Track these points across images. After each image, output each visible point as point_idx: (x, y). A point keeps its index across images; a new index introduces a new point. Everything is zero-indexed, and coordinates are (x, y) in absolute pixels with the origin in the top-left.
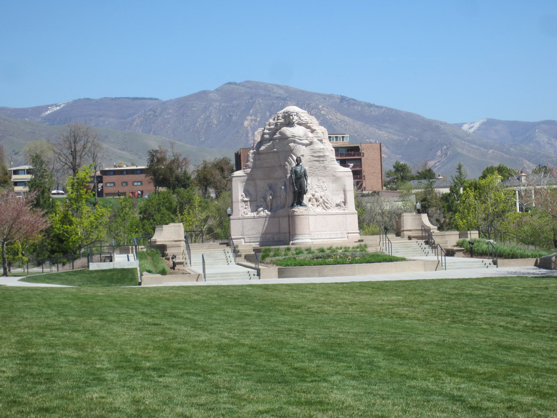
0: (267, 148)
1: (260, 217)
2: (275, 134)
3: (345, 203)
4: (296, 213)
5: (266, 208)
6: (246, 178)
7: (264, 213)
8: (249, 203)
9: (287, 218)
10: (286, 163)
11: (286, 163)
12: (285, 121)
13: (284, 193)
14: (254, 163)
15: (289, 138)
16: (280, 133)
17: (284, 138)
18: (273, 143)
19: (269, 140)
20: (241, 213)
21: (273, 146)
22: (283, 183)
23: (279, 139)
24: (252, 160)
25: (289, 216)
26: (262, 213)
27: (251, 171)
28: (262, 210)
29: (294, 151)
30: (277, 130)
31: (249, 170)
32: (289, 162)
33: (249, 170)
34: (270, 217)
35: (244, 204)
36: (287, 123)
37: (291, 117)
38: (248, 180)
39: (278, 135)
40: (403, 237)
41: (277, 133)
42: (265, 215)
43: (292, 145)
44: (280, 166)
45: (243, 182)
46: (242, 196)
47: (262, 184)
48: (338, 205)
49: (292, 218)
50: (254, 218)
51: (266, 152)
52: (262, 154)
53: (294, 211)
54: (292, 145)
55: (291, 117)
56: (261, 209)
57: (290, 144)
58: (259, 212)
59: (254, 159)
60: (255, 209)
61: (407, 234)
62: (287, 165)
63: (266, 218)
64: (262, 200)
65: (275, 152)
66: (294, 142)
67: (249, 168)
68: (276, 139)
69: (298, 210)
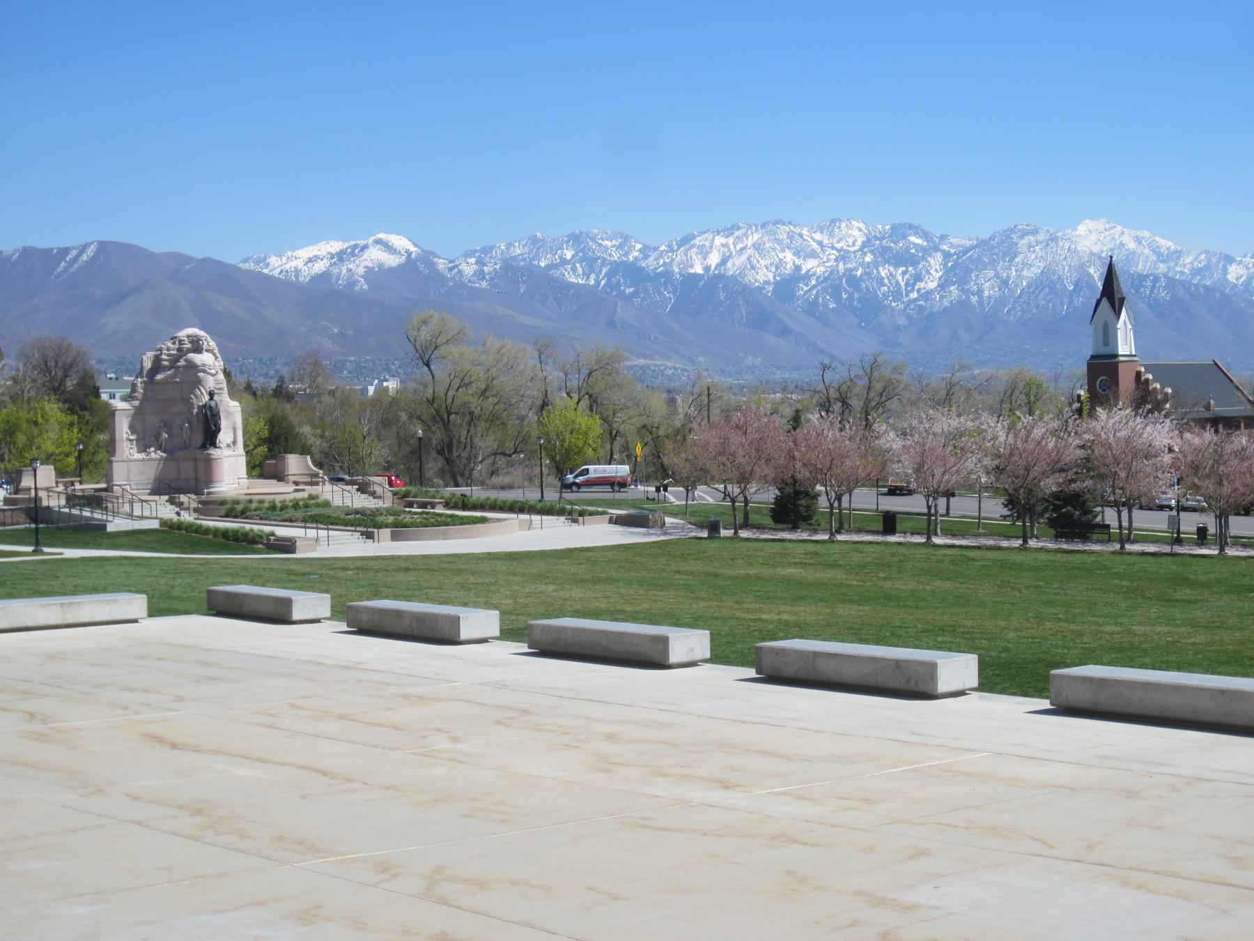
0: (166, 378)
1: (151, 460)
2: (178, 360)
3: (234, 443)
5: (159, 448)
7: (155, 454)
14: (144, 395)
16: (186, 360)
17: (192, 366)
19: (170, 368)
20: (127, 453)
21: (175, 376)
23: (184, 367)
30: (181, 357)
31: (137, 403)
34: (166, 460)
39: (182, 363)
40: (287, 482)
43: (201, 374)
47: (153, 420)
48: (228, 445)
49: (209, 461)
50: (143, 460)
51: (164, 382)
54: (201, 374)
58: (149, 453)
59: (145, 389)
60: (143, 448)
61: (292, 478)
66: (204, 371)
69: (214, 452)
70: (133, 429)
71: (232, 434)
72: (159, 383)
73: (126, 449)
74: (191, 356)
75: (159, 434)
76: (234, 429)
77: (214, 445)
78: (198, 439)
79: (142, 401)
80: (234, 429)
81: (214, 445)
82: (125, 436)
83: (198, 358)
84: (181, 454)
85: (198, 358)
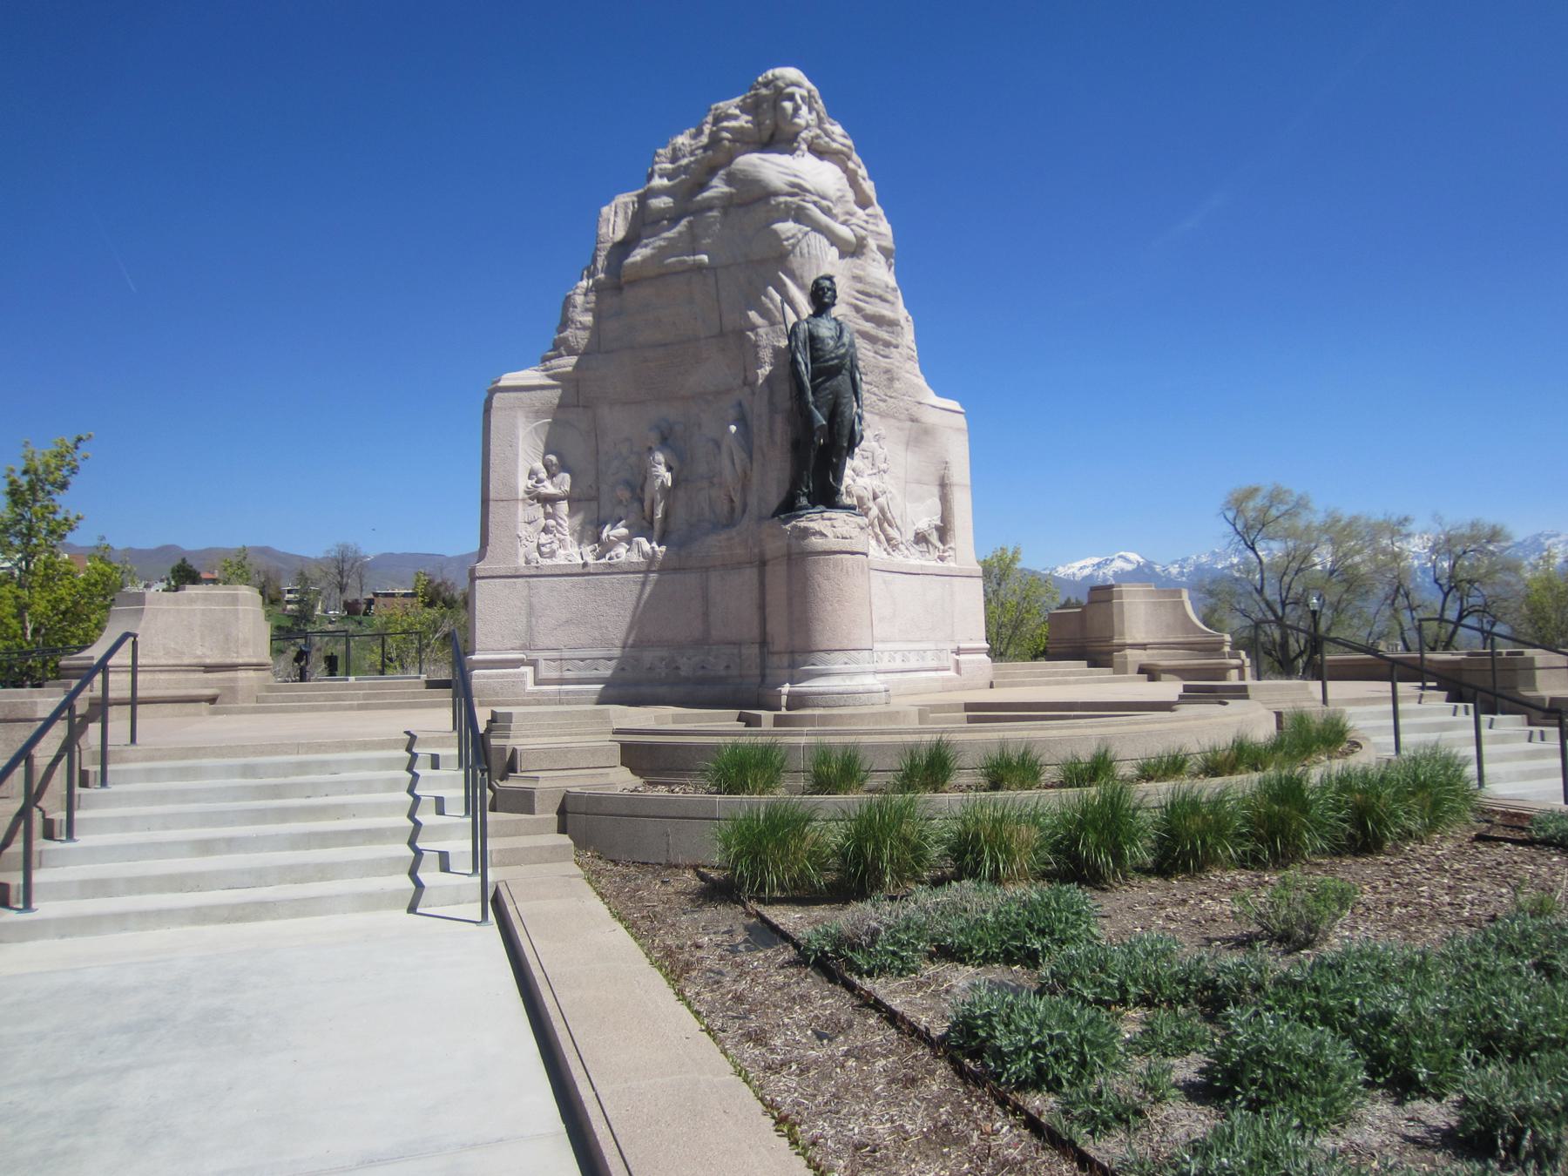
0: (662, 253)
1: (612, 570)
2: (703, 186)
3: (944, 531)
4: (816, 541)
5: (643, 527)
6: (554, 396)
7: (634, 550)
8: (563, 506)
9: (751, 574)
10: (753, 314)
11: (753, 314)
12: (758, 124)
13: (739, 456)
14: (596, 330)
15: (776, 194)
16: (730, 180)
17: (755, 198)
18: (691, 225)
19: (675, 221)
20: (526, 550)
22: (732, 413)
23: (727, 204)
24: (588, 319)
25: (763, 563)
26: (622, 550)
27: (577, 367)
28: (620, 539)
29: (795, 262)
30: (712, 172)
31: (568, 363)
32: (765, 313)
33: (568, 363)
35: (538, 511)
36: (766, 135)
37: (788, 105)
38: (562, 405)
39: (718, 187)
40: (1122, 669)
41: (716, 182)
42: (635, 557)
43: (787, 228)
44: (722, 334)
45: (538, 414)
46: (532, 474)
48: (921, 538)
49: (800, 560)
50: (584, 571)
51: (656, 274)
52: (633, 283)
53: (806, 533)
54: (787, 228)
55: (788, 105)
56: (621, 531)
57: (778, 226)
58: (605, 547)
59: (598, 315)
60: (591, 532)
61: (1135, 657)
62: (754, 328)
63: (647, 572)
64: (624, 494)
65: (699, 267)
66: (800, 216)
67: (571, 352)
68: (709, 206)
70: (558, 455)
71: (934, 504)
72: (640, 278)
74: (751, 161)
75: (645, 475)
76: (944, 485)
77: (828, 497)
79: (585, 355)
80: (944, 485)
81: (828, 497)
82: (523, 483)
83: (772, 168)
84: (715, 544)
85: (772, 168)
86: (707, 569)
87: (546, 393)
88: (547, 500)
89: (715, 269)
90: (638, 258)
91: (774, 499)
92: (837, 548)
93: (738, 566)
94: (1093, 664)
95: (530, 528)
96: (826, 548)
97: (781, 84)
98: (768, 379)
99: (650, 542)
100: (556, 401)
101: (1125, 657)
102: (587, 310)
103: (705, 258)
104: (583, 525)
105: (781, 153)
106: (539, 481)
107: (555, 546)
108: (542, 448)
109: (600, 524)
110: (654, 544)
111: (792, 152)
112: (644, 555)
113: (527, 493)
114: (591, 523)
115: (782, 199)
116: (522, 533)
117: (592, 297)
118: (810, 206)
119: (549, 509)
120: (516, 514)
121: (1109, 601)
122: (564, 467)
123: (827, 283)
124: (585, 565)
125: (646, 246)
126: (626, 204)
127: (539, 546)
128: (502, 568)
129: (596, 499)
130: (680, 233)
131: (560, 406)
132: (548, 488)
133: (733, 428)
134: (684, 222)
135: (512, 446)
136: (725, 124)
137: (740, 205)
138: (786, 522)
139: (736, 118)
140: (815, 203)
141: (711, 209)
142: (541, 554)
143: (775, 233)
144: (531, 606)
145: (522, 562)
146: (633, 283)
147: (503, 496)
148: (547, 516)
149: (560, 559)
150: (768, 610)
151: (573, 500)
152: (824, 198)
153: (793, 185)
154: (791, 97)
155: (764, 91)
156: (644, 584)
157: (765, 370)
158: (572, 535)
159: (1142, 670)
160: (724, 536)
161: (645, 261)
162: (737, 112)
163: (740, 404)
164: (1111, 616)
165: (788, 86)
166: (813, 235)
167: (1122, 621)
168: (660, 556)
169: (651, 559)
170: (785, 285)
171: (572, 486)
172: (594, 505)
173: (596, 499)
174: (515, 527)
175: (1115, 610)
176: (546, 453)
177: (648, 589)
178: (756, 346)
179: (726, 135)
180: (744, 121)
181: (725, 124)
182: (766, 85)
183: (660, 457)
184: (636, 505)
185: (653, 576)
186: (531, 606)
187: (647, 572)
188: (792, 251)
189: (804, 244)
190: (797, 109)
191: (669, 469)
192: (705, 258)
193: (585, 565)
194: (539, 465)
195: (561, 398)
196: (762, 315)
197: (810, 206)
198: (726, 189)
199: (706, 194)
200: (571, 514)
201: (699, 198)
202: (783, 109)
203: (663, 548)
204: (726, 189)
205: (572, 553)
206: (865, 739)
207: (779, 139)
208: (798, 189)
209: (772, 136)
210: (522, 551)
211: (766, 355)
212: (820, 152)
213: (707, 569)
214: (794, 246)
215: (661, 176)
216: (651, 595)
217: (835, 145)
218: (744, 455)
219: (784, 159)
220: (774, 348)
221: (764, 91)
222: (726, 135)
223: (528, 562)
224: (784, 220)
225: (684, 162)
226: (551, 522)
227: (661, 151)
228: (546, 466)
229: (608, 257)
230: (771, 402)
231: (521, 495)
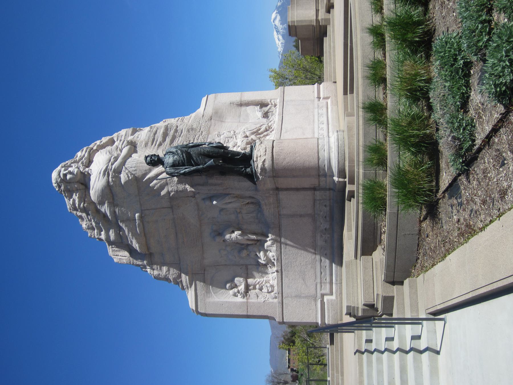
1: (279, 259)
2: (105, 215)
3: (263, 105)
4: (267, 164)
5: (260, 244)
6: (200, 284)
7: (271, 249)
8: (250, 281)
9: (282, 195)
10: (163, 193)
11: (163, 193)
12: (77, 190)
13: (227, 200)
14: (170, 265)
15: (108, 182)
16: (102, 203)
17: (110, 192)
19: (120, 229)
22: (208, 203)
23: (113, 204)
24: (165, 269)
25: (277, 189)
26: (270, 254)
27: (186, 274)
28: (265, 255)
29: (139, 174)
30: (98, 211)
31: (185, 278)
32: (162, 188)
33: (185, 278)
34: (279, 234)
35: (252, 293)
36: (82, 187)
37: (69, 177)
39: (105, 209)
40: (328, 21)
41: (103, 210)
42: (274, 248)
43: (123, 178)
44: (171, 207)
45: (208, 292)
46: (235, 295)
48: (266, 115)
49: (276, 172)
50: (280, 272)
51: (144, 237)
52: (148, 249)
53: (263, 169)
54: (123, 178)
55: (69, 177)
56: (262, 254)
57: (123, 182)
58: (269, 262)
60: (262, 268)
61: (322, 14)
62: (169, 193)
63: (281, 243)
64: (244, 253)
65: (141, 217)
66: (118, 171)
67: (180, 276)
68: (114, 213)
69: (261, 159)
70: (225, 283)
71: (250, 109)
73: (261, 299)
74: (94, 193)
76: (242, 104)
77: (246, 159)
78: (237, 184)
79: (181, 270)
80: (242, 104)
81: (246, 159)
82: (239, 299)
83: (97, 184)
84: (268, 212)
85: (97, 184)
86: (279, 215)
87: (198, 288)
88: (247, 288)
89: (142, 210)
90: (137, 245)
91: (247, 184)
92: (271, 154)
93: (278, 201)
94: (325, 34)
95: (260, 296)
96: (270, 159)
97: (59, 180)
98: (192, 186)
99: (266, 241)
100: (202, 283)
101: (322, 19)
102: (161, 269)
103: (137, 215)
104: (259, 272)
105: (90, 180)
106: (238, 292)
107: (268, 285)
108: (223, 290)
109: (258, 264)
110: (268, 239)
111: (90, 175)
112: (273, 244)
113: (244, 297)
114: (258, 268)
115: (110, 180)
116: (263, 300)
117: (155, 267)
118: (113, 167)
119: (251, 287)
120: (253, 303)
121: (296, 27)
122: (232, 281)
123: (148, 159)
124: (277, 271)
125: (132, 242)
126: (113, 251)
127: (268, 292)
128: (278, 310)
129: (247, 266)
130: (126, 226)
131: (204, 282)
132: (242, 288)
133: (215, 202)
134: (121, 224)
135: (222, 304)
136: (77, 205)
137: (113, 199)
138: (258, 178)
139: (74, 201)
140: (112, 164)
141: (115, 212)
142: (272, 291)
143: (126, 182)
144: (296, 296)
145: (276, 300)
146: (148, 249)
147: (245, 308)
148: (255, 288)
149: (275, 283)
150: (299, 187)
151: (247, 277)
152: (110, 160)
153: (104, 174)
154: (65, 175)
155: (62, 188)
156: (286, 244)
157: (188, 188)
158: (263, 277)
159: (328, 11)
160: (264, 207)
161: (138, 242)
162: (72, 200)
163: (204, 199)
164: (302, 26)
165: (60, 177)
166: (126, 166)
167: (305, 21)
168: (273, 237)
169: (274, 241)
170: (149, 178)
171: (241, 277)
172: (249, 267)
173: (247, 266)
174: (259, 303)
175: (300, 24)
176: (226, 288)
177: (289, 242)
178: (177, 192)
179: (82, 205)
180: (76, 197)
181: (77, 205)
182: (60, 187)
183: (227, 236)
184: (250, 248)
185: (283, 240)
186: (296, 296)
187: (281, 243)
188: (134, 175)
189: (131, 170)
190: (70, 173)
191: (233, 232)
192: (137, 215)
193: (277, 271)
194: (231, 292)
195: (201, 281)
196: (163, 189)
197: (113, 167)
198: (106, 205)
199: (108, 214)
200: (253, 277)
201: (110, 217)
202: (70, 179)
203: (270, 235)
204: (106, 205)
205: (271, 277)
206: (361, 143)
207: (84, 181)
208: (106, 172)
209: (82, 184)
210: (271, 300)
211: (181, 187)
212: (90, 162)
213: (279, 215)
214: (132, 174)
215: (100, 235)
216: (291, 241)
217: (86, 155)
218: (227, 198)
219: (93, 178)
220: (177, 183)
221: (62, 188)
222: (82, 205)
223: (276, 298)
224: (120, 178)
225: (94, 224)
226: (257, 286)
227: (89, 235)
228: (232, 289)
229: (137, 259)
230: (203, 185)
231: (245, 300)
